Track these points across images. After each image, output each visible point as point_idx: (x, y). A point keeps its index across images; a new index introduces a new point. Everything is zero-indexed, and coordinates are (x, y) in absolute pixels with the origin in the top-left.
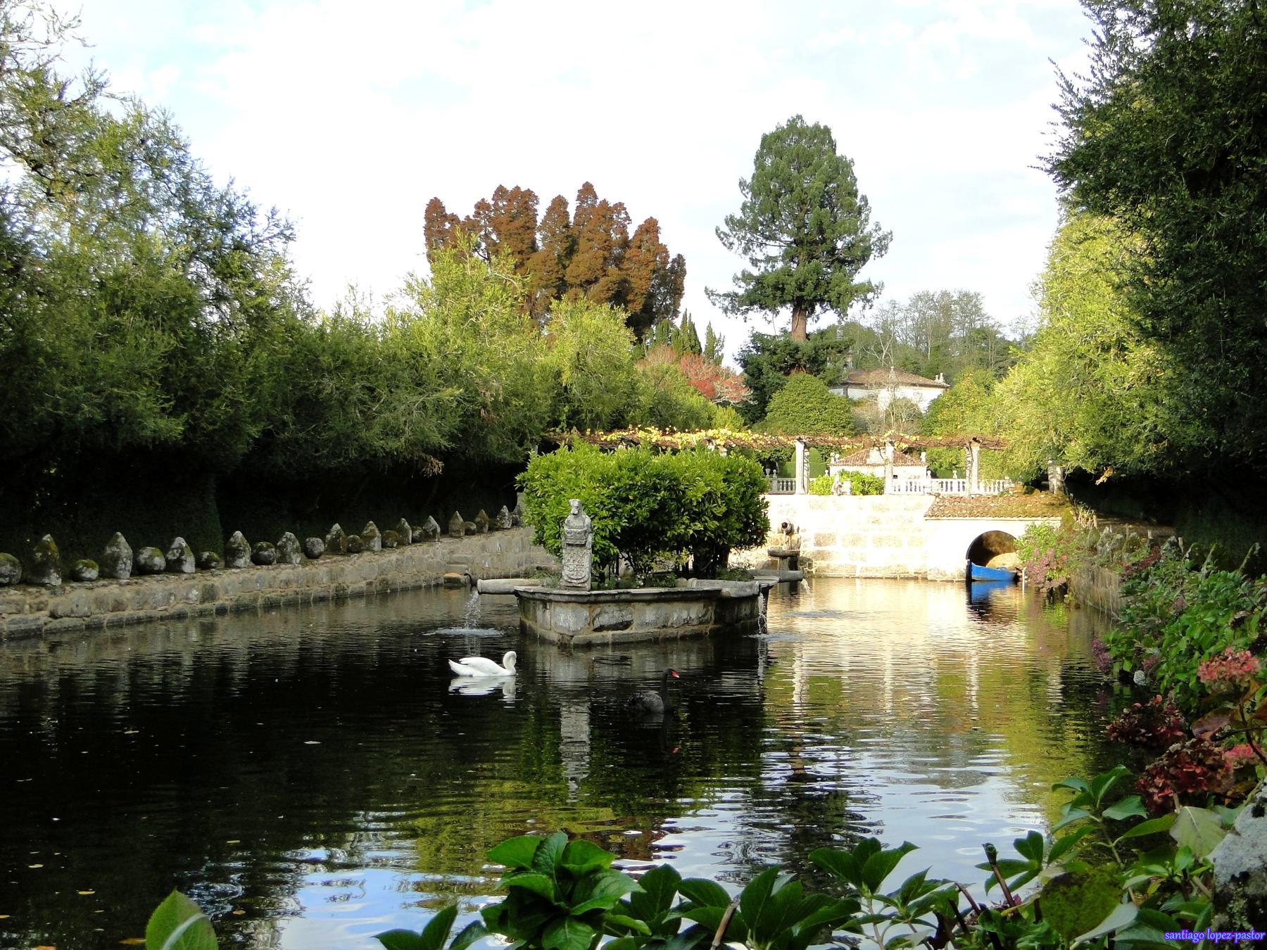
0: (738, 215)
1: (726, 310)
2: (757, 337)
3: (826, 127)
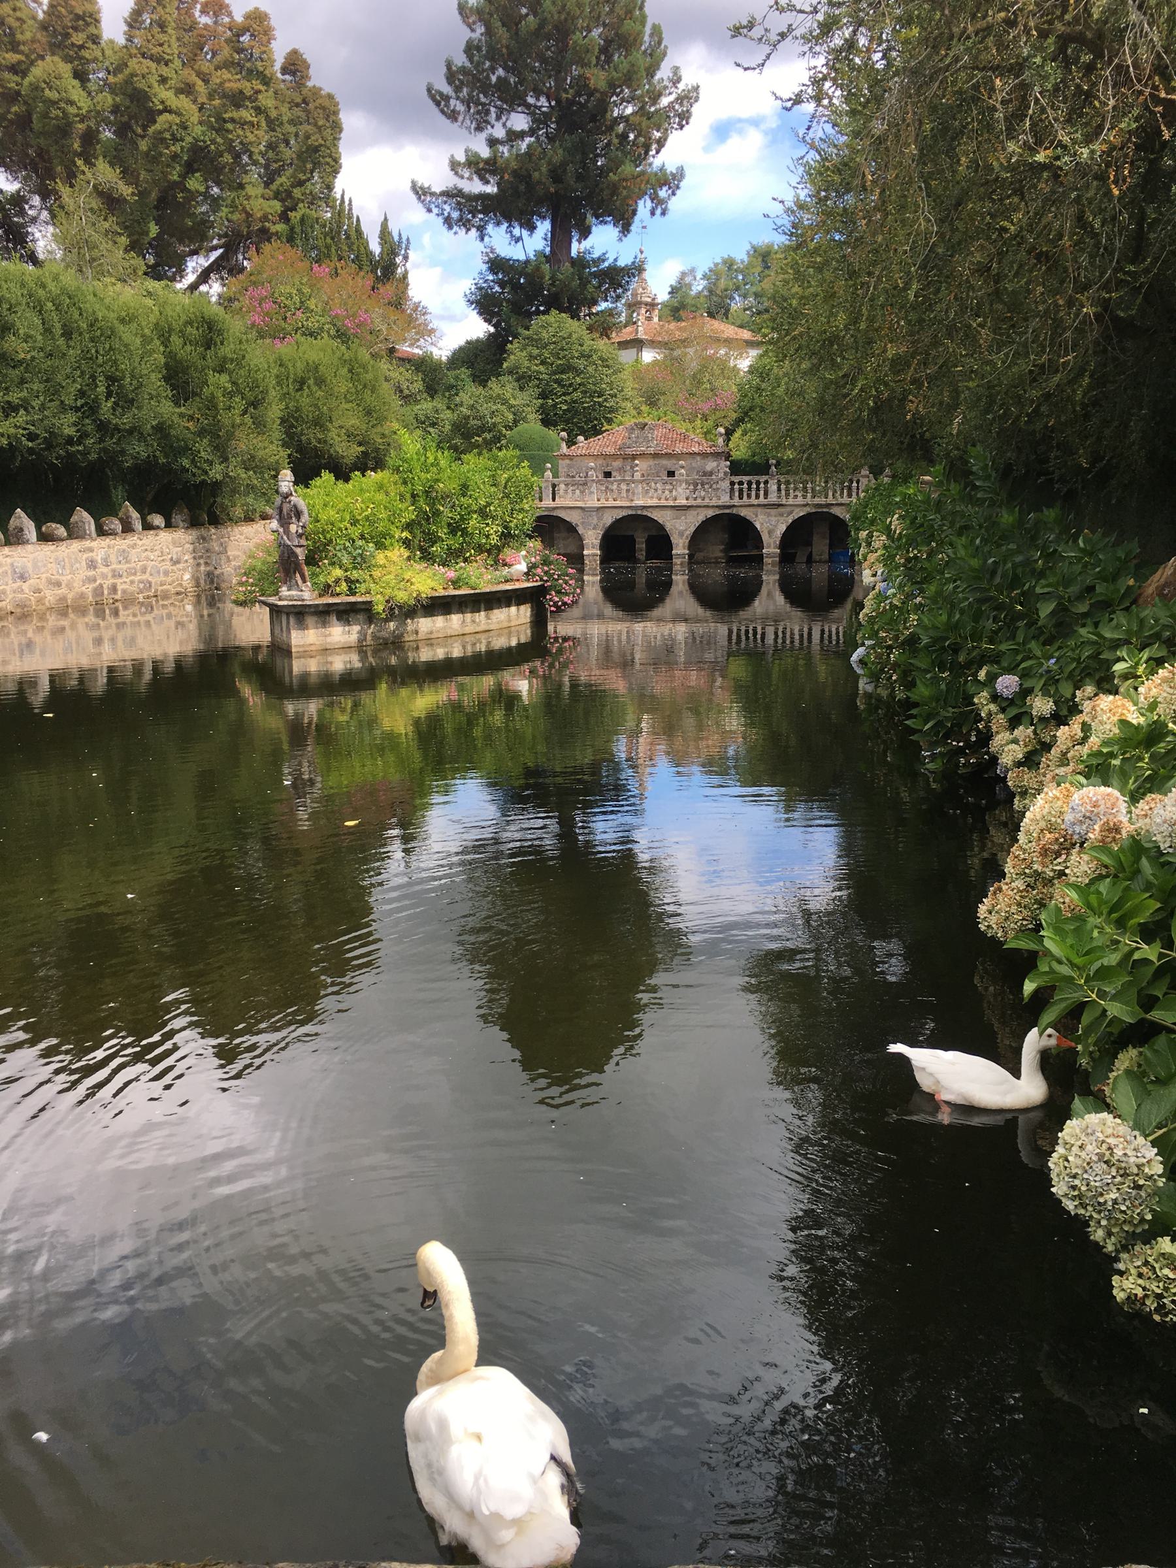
0: (461, 60)
1: (448, 222)
2: (496, 264)
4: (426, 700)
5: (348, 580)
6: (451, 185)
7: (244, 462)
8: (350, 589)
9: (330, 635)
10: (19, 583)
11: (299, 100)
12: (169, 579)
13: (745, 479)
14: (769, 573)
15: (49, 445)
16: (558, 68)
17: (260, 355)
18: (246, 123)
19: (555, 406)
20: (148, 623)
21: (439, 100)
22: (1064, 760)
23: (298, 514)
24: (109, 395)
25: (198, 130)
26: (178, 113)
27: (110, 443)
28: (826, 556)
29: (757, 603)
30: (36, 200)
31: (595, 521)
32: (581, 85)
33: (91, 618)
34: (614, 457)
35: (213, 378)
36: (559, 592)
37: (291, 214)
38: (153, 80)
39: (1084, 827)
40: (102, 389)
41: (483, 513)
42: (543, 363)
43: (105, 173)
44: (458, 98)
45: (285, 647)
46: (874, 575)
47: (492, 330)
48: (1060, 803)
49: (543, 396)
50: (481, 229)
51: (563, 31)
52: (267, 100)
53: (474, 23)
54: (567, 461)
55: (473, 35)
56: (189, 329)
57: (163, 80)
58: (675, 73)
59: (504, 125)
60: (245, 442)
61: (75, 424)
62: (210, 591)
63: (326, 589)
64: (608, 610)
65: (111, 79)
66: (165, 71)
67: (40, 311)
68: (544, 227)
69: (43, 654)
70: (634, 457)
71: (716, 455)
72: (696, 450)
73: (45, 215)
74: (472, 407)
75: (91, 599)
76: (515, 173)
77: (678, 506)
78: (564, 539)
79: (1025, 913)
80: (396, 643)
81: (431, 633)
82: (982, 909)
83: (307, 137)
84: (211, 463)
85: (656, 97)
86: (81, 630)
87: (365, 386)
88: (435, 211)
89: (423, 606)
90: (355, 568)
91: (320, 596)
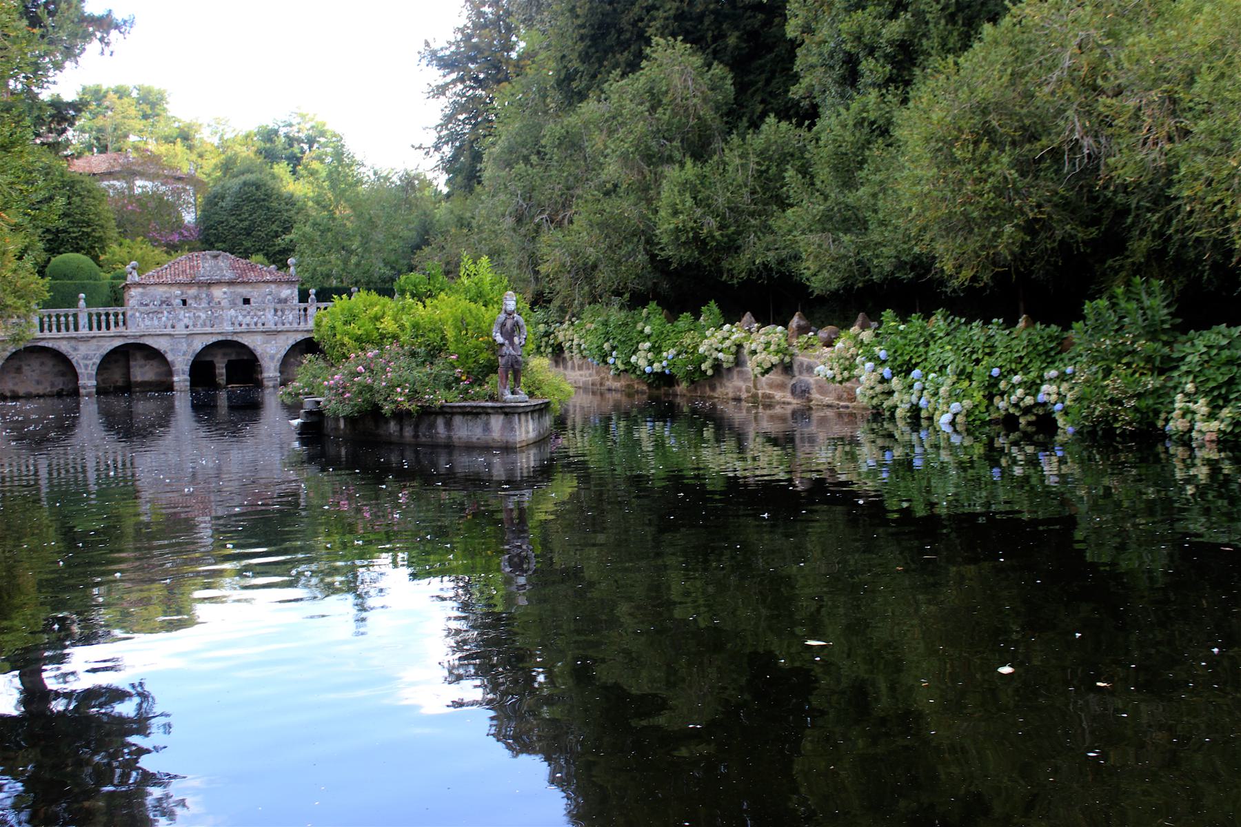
31: (184, 347)
54: (140, 290)
70: (209, 285)
71: (290, 283)
78: (141, 367)
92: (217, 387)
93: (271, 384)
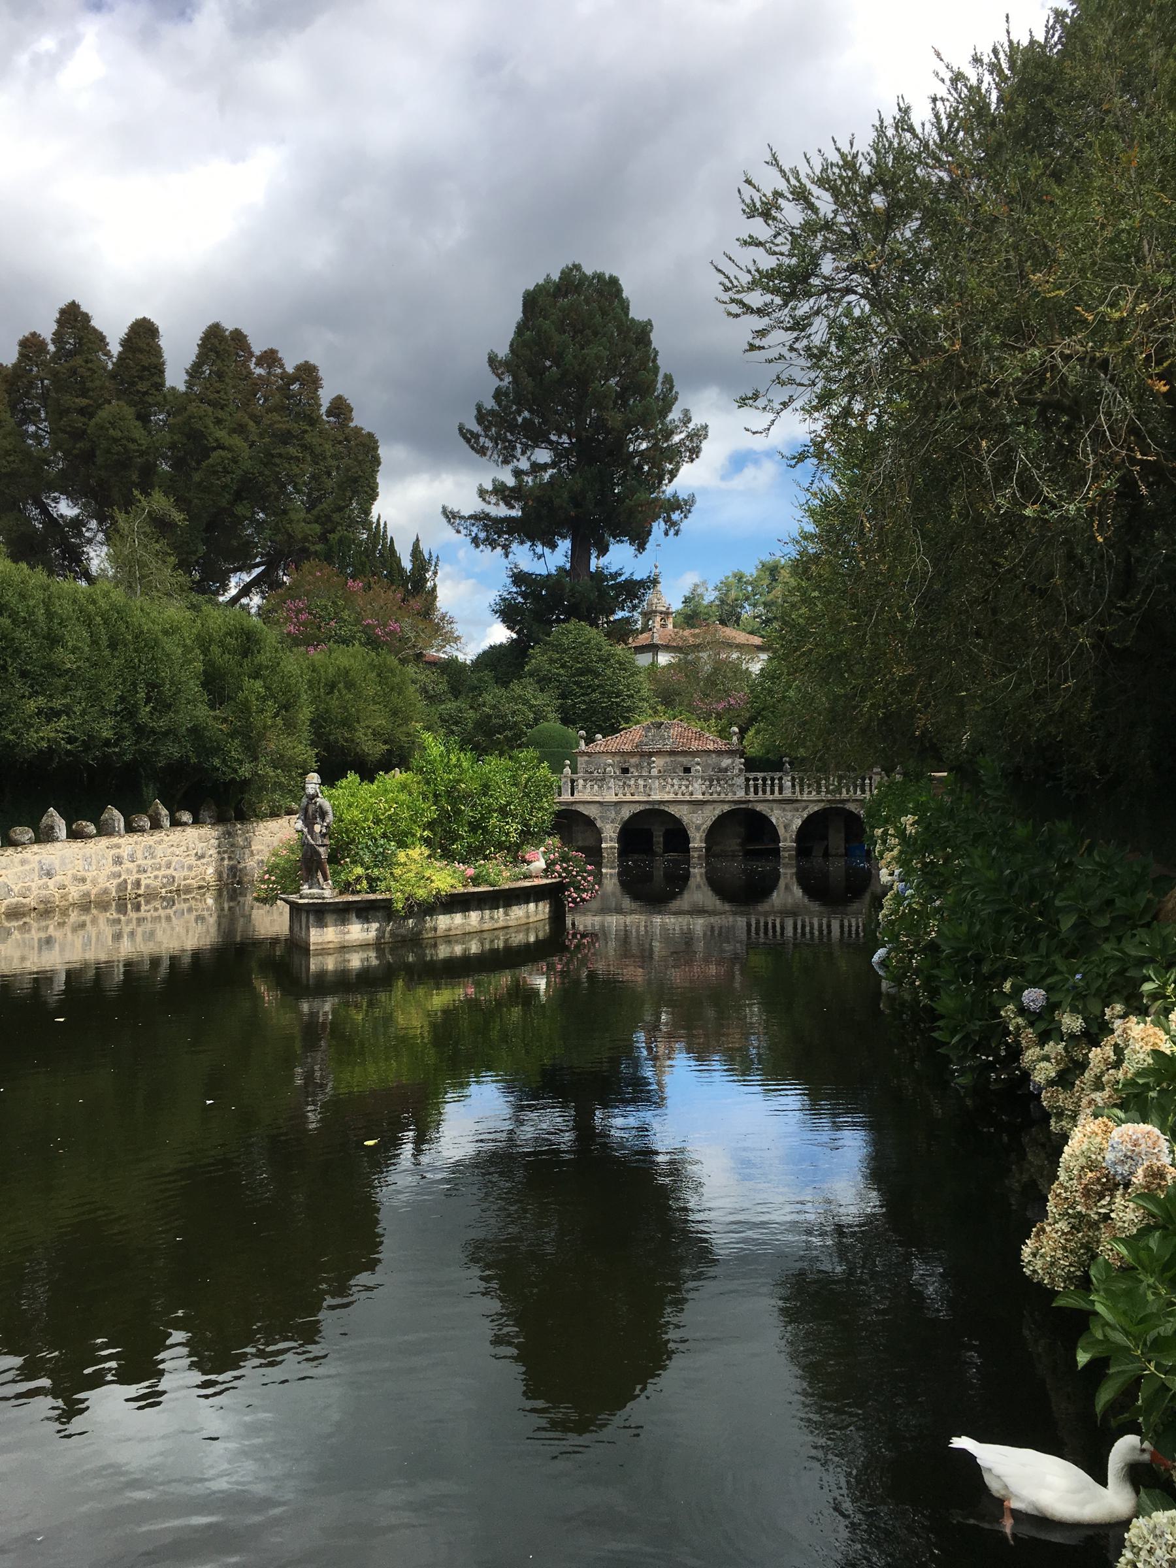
0: (490, 404)
1: (476, 541)
2: (519, 578)
3: (611, 277)
4: (441, 999)
5: (370, 879)
6: (479, 510)
7: (272, 761)
8: (371, 887)
9: (348, 932)
10: (45, 879)
11: (341, 438)
12: (193, 874)
13: (760, 775)
14: (786, 866)
15: (87, 746)
16: (579, 411)
17: (293, 663)
18: (292, 458)
19: (574, 705)
20: (168, 918)
21: (468, 437)
22: (1098, 1086)
23: (323, 814)
24: (148, 700)
25: (247, 464)
26: (230, 449)
27: (145, 744)
28: (842, 850)
29: (775, 894)
30: (93, 524)
31: (613, 815)
32: (599, 424)
33: (113, 914)
34: (631, 754)
35: (247, 683)
36: (577, 889)
37: (331, 536)
38: (209, 422)
39: (1126, 1168)
40: (142, 695)
41: (503, 812)
42: (563, 666)
43: (160, 502)
44: (487, 436)
45: (303, 945)
46: (891, 874)
47: (515, 636)
48: (1099, 1139)
49: (563, 696)
50: (506, 547)
51: (582, 381)
52: (311, 438)
53: (503, 373)
54: (586, 758)
55: (502, 384)
56: (228, 639)
57: (219, 422)
58: (686, 415)
59: (529, 459)
60: (274, 743)
61: (113, 728)
62: (232, 884)
63: (346, 887)
64: (627, 903)
65: (171, 420)
66: (220, 414)
67: (89, 625)
68: (565, 545)
69: (62, 950)
70: (651, 754)
71: (731, 753)
72: (711, 748)
73: (101, 536)
74: (494, 707)
75: (114, 894)
76: (538, 499)
77: (695, 798)
79: (1072, 1258)
80: (414, 941)
81: (450, 930)
82: (1026, 1251)
83: (348, 470)
84: (241, 762)
85: (669, 434)
86: (102, 926)
87: (392, 690)
88: (464, 532)
89: (442, 903)
90: (376, 866)
91: (341, 893)
92: (654, 854)
93: (696, 854)
